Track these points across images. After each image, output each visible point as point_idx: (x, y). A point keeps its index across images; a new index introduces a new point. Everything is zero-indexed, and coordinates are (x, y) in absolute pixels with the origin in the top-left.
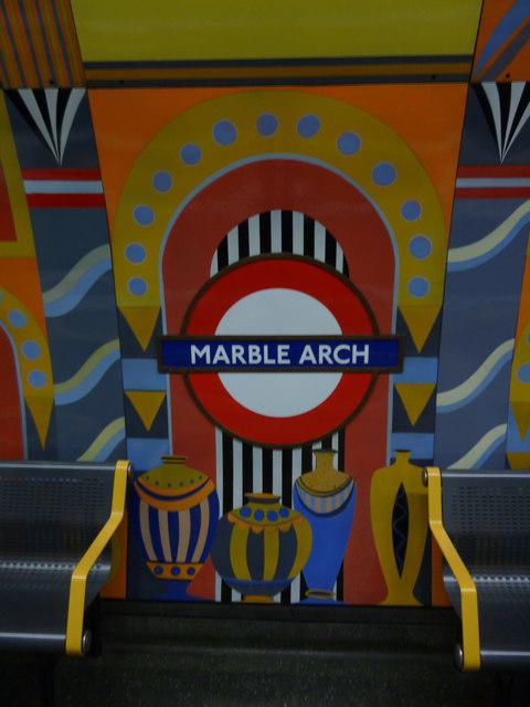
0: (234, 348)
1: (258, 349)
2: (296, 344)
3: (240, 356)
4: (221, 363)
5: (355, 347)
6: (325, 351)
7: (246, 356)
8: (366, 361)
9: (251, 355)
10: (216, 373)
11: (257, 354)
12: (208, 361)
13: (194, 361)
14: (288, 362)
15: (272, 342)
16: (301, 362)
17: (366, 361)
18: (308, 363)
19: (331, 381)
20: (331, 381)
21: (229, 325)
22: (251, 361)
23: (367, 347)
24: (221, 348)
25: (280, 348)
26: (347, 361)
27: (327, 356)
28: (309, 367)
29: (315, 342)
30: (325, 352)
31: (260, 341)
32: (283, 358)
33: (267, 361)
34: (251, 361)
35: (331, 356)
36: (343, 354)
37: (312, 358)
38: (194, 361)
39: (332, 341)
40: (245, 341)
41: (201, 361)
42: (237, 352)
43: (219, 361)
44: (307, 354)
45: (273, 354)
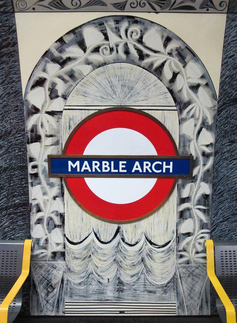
0: (94, 162)
1: (108, 163)
3: (97, 167)
4: (86, 171)
5: (164, 163)
6: (147, 165)
7: (100, 167)
8: (171, 171)
9: (104, 166)
10: (83, 178)
11: (107, 166)
12: (78, 170)
13: (70, 170)
14: (125, 171)
15: (116, 160)
16: (133, 171)
17: (171, 171)
18: (137, 172)
19: (151, 182)
20: (151, 182)
21: (92, 149)
22: (104, 170)
23: (171, 163)
24: (86, 163)
25: (121, 163)
26: (160, 171)
27: (148, 168)
28: (137, 175)
29: (141, 159)
30: (147, 166)
31: (109, 159)
32: (123, 169)
33: (113, 171)
34: (104, 170)
35: (151, 168)
36: (159, 167)
37: (139, 169)
38: (70, 170)
39: (151, 159)
40: (100, 159)
41: (74, 170)
42: (96, 165)
44: (137, 166)
45: (116, 167)
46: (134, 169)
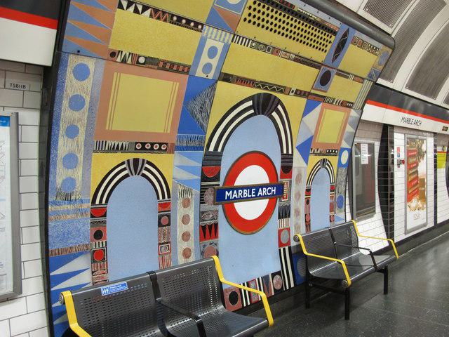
2: (258, 187)
7: (242, 194)
9: (244, 193)
15: (249, 188)
20: (265, 202)
21: (238, 183)
24: (235, 191)
25: (253, 190)
29: (262, 186)
39: (266, 186)
40: (243, 188)
41: (228, 197)
43: (235, 198)
45: (250, 194)
46: (259, 194)
